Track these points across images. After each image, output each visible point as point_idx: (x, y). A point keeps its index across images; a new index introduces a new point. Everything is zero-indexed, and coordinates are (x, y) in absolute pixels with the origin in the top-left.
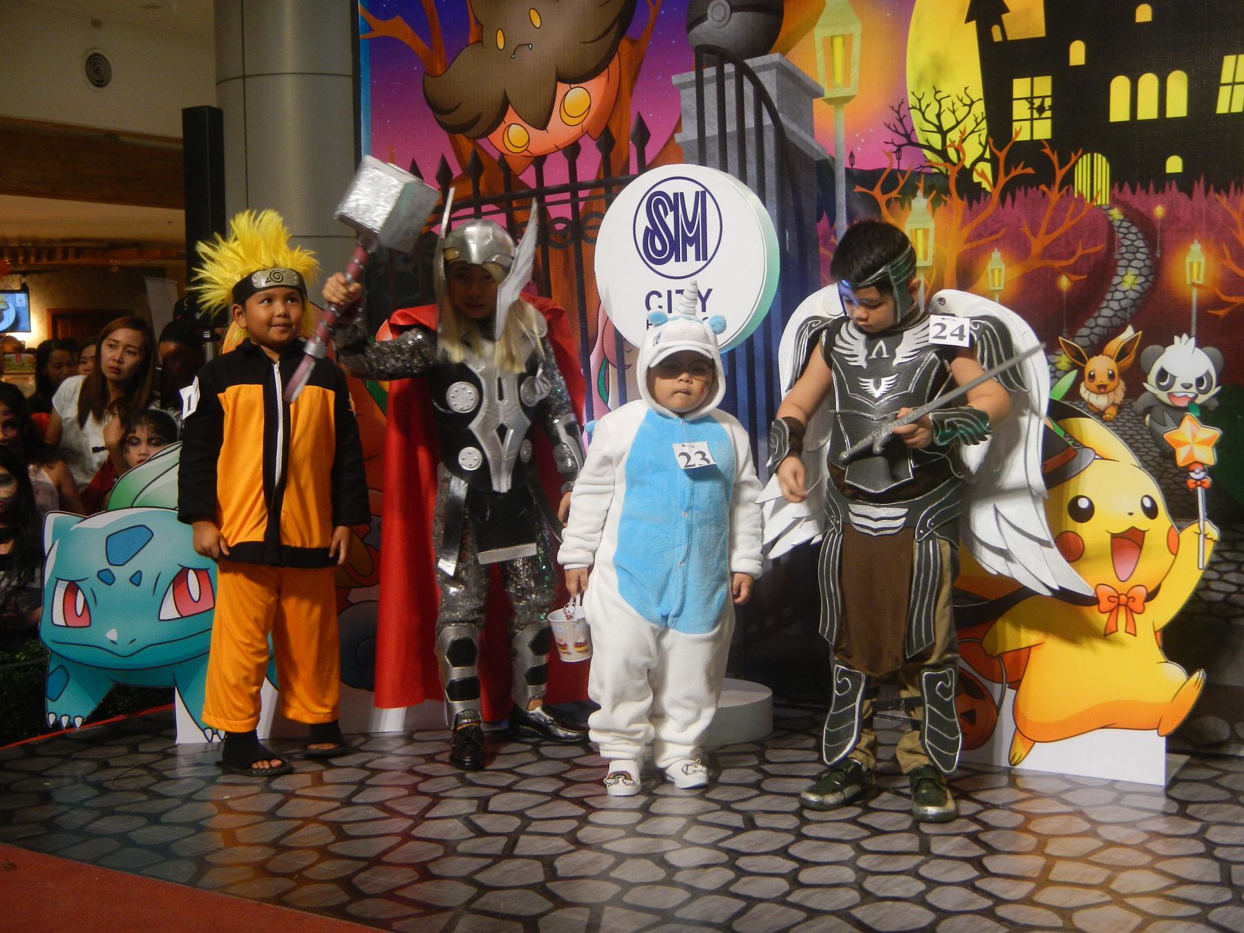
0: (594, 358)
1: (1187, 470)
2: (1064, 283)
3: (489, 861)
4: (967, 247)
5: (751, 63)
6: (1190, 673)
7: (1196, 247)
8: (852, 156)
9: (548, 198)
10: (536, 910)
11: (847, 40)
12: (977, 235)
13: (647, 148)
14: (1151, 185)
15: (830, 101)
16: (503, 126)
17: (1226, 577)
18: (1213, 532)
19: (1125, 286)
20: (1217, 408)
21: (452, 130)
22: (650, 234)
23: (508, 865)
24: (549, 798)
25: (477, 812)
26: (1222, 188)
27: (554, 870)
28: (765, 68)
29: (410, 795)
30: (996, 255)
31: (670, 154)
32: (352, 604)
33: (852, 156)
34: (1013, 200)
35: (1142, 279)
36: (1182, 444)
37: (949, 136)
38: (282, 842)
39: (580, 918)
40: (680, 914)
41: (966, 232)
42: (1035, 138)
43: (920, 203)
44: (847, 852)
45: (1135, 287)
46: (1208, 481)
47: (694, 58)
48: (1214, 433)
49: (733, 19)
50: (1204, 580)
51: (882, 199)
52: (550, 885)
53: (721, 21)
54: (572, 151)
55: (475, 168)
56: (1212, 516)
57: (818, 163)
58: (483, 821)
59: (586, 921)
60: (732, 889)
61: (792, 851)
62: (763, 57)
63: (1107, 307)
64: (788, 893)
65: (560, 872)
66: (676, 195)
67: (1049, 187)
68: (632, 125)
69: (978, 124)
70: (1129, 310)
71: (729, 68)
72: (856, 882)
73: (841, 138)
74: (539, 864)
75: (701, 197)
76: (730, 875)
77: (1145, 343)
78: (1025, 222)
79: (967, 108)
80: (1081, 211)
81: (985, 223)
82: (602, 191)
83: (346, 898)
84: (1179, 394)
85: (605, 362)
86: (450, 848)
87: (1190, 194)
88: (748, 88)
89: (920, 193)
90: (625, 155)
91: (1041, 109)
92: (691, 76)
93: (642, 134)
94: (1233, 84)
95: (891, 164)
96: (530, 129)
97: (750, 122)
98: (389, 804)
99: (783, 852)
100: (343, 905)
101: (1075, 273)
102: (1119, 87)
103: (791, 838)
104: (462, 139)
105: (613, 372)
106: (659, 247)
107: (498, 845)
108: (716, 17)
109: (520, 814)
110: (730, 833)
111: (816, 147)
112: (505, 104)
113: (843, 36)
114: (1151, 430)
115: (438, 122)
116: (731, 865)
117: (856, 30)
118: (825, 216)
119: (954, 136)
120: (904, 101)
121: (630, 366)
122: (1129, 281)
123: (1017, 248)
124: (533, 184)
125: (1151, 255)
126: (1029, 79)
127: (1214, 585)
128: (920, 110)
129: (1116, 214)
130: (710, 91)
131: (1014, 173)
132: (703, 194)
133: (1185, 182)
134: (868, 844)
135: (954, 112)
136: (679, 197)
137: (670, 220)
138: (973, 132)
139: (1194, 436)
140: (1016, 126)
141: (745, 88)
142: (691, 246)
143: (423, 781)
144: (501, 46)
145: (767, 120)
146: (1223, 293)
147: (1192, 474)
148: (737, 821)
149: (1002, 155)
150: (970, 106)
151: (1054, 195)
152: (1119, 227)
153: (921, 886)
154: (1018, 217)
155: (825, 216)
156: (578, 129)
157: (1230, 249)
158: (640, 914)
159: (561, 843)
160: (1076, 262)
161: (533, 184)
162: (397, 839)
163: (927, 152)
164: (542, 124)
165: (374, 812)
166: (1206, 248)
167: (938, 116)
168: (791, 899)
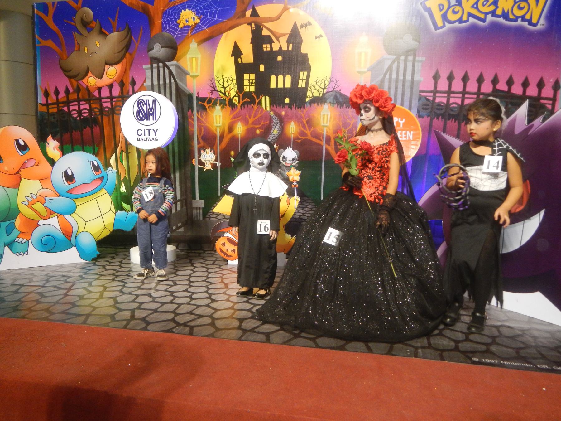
0: (118, 150)
1: (292, 183)
2: (258, 132)
3: (95, 300)
4: (232, 120)
5: (168, 63)
6: (292, 237)
7: (293, 123)
8: (198, 93)
9: (103, 101)
10: (114, 313)
11: (197, 59)
12: (234, 117)
13: (135, 87)
14: (281, 106)
15: (192, 76)
16: (87, 77)
17: (299, 211)
18: (298, 199)
19: (274, 133)
20: (298, 167)
21: (70, 77)
22: (139, 112)
23: (101, 301)
24: (111, 281)
25: (89, 286)
26: (300, 107)
27: (117, 301)
28: (172, 65)
29: (64, 283)
30: (239, 123)
31: (142, 88)
32: (40, 225)
33: (198, 93)
34: (244, 108)
35: (279, 131)
36: (291, 175)
37: (226, 89)
38: (22, 300)
39: (128, 314)
40: (159, 310)
41: (231, 116)
42: (250, 91)
43: (218, 107)
44: (205, 289)
46: (297, 185)
48: (299, 172)
49: (162, 50)
50: (295, 212)
51: (207, 106)
52: (117, 305)
54: (111, 86)
55: (78, 90)
56: (298, 195)
57: (188, 94)
58: (90, 289)
59: (130, 314)
60: (173, 302)
61: (189, 290)
63: (269, 139)
64: (190, 301)
65: (119, 302)
66: (146, 100)
67: (254, 105)
68: (130, 80)
69: (234, 86)
71: (161, 65)
72: (209, 297)
73: (195, 87)
74: (111, 299)
75: (155, 101)
76: (172, 298)
77: (279, 149)
78: (247, 114)
79: (231, 81)
80: (262, 112)
81: (236, 114)
82: (120, 99)
83: (48, 315)
84: (288, 163)
85: (122, 151)
86: (81, 297)
87: (291, 108)
88: (167, 71)
89: (218, 105)
90: (128, 89)
91: (252, 83)
92: (149, 66)
93: (134, 83)
94: (303, 79)
95: (210, 95)
96: (96, 78)
97: (167, 81)
98: (58, 286)
99: (186, 290)
100: (48, 317)
101: (261, 129)
102: (273, 78)
103: (188, 287)
104: (73, 80)
105: (124, 154)
106: (141, 116)
107: (98, 295)
109: (103, 286)
110: (170, 286)
111: (188, 90)
112: (88, 70)
113: (195, 58)
114: (281, 173)
115: (64, 74)
116: (172, 295)
117: (199, 56)
118: (190, 110)
119: (228, 89)
120: (213, 78)
121: (130, 153)
122: (275, 132)
123: (246, 122)
124: (98, 96)
125: (281, 125)
126: (248, 74)
127: (297, 214)
128: (218, 81)
129: (272, 113)
130: (155, 71)
131: (244, 100)
132: (155, 101)
133: (290, 105)
134: (210, 287)
135: (228, 82)
136: (147, 101)
137: (144, 108)
138: (233, 88)
139: (294, 173)
140: (245, 87)
141: (166, 71)
143: (68, 278)
144: (86, 52)
145: (173, 81)
146: (300, 135)
147: (293, 183)
148: (171, 283)
149: (241, 95)
150: (232, 81)
151: (255, 107)
152: (273, 117)
153: (228, 297)
154: (246, 114)
155: (190, 110)
156: (112, 80)
157: (301, 124)
158: (147, 311)
159: (118, 293)
160: (261, 126)
161: (98, 96)
162: (62, 296)
163: (220, 93)
164: (101, 77)
165: (53, 289)
166: (295, 124)
167: (223, 83)
168: (192, 302)
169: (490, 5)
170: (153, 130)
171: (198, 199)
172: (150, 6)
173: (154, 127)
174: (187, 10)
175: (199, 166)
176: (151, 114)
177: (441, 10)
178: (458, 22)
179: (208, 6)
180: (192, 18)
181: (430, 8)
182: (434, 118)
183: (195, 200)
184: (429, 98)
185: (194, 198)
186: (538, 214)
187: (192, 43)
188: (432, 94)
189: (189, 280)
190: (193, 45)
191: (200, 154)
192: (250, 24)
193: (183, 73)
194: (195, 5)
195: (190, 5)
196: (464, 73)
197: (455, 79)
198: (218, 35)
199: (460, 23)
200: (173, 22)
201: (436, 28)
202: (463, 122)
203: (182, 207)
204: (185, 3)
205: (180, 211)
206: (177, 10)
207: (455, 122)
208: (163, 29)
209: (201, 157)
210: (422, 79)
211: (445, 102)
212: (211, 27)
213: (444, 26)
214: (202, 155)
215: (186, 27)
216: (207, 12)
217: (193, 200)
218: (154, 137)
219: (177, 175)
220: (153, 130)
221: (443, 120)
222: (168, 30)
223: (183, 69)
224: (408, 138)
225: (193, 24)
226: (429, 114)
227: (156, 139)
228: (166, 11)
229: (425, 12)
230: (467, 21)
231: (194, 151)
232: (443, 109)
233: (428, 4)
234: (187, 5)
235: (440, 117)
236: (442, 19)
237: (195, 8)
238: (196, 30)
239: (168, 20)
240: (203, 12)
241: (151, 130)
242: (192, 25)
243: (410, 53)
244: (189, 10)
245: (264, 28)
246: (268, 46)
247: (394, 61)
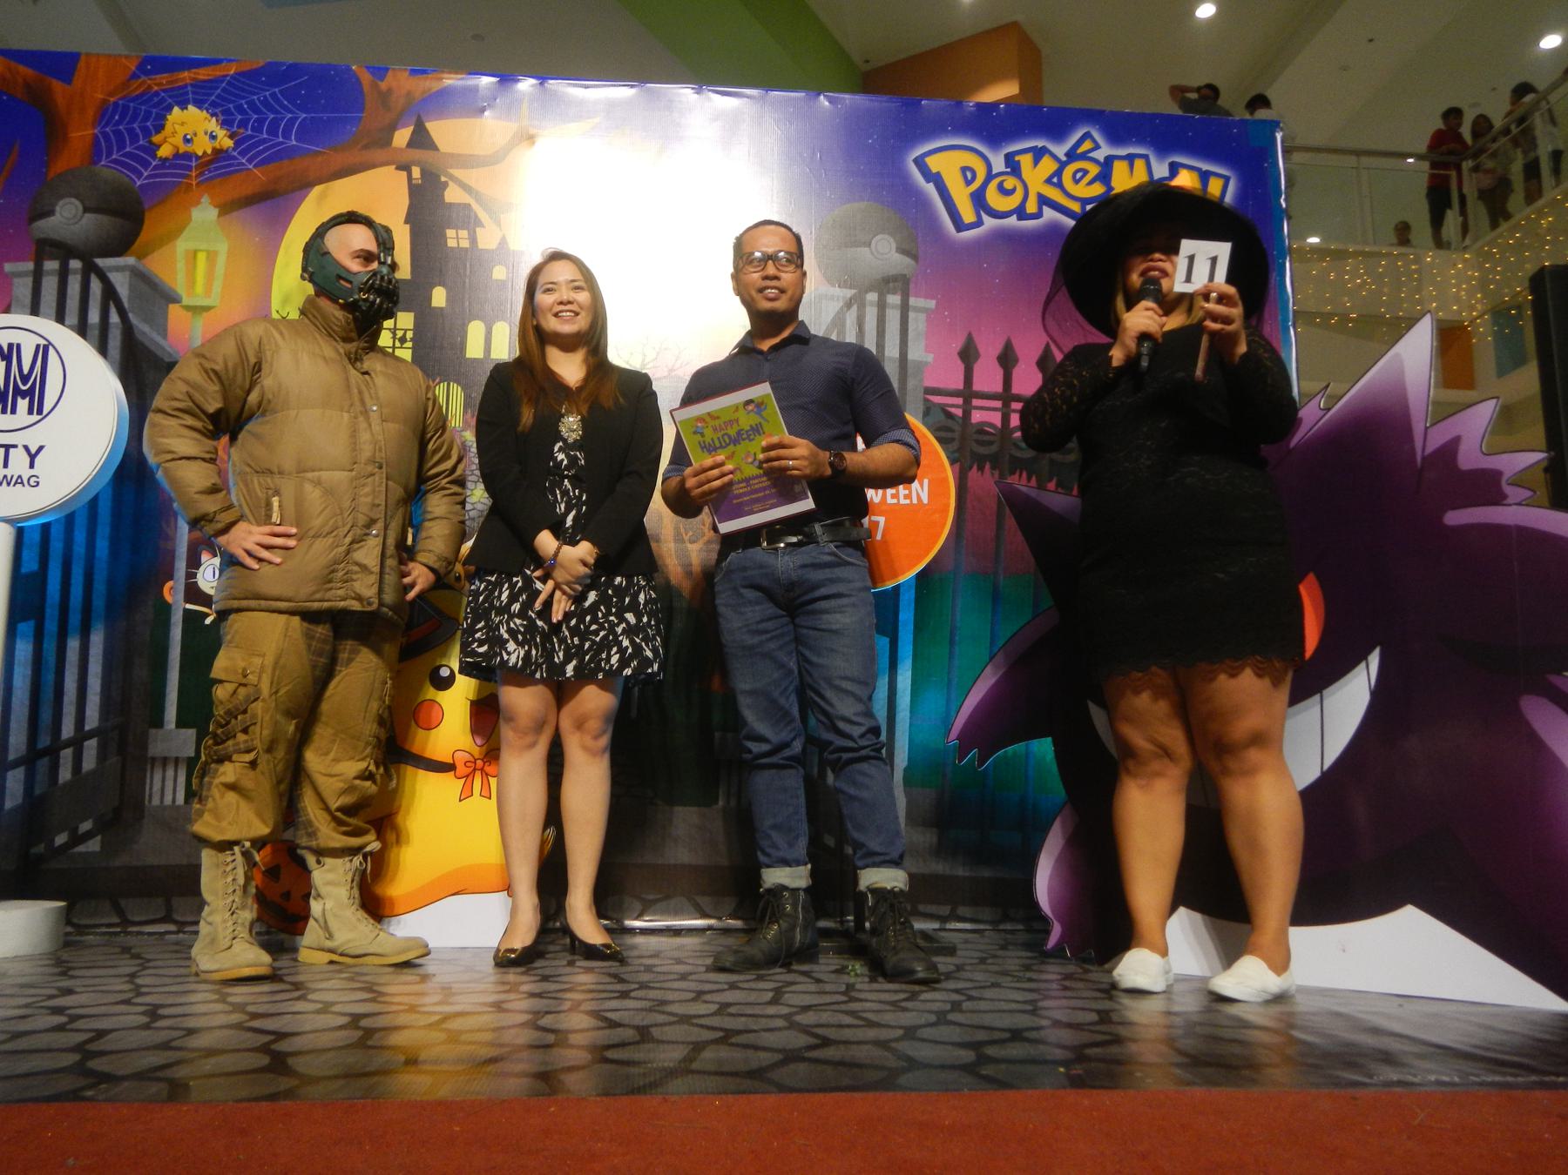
5: (100, 262)
11: (212, 257)
15: (188, 308)
28: (118, 269)
45: (482, 500)
47: (34, 248)
49: (84, 221)
53: (67, 219)
62: (117, 259)
66: (10, 346)
70: (477, 520)
75: (43, 351)
88: (96, 286)
92: (30, 266)
97: (94, 317)
99: (127, 1002)
102: (475, 331)
108: (65, 214)
111: (168, 349)
113: (208, 252)
117: (222, 248)
132: (46, 349)
141: (92, 285)
142: (23, 398)
145: (114, 318)
169: (1091, 183)
170: (26, 448)
171: (173, 726)
172: (57, 86)
173: (32, 439)
174: (191, 107)
175: (189, 606)
176: (24, 394)
177: (968, 183)
178: (1015, 216)
179: (265, 103)
180: (206, 133)
181: (938, 174)
182: (971, 468)
183: (160, 732)
184: (953, 410)
185: (158, 722)
186: (1363, 665)
187: (199, 206)
188: (960, 401)
189: (132, 982)
190: (204, 213)
191: (194, 563)
192: (405, 167)
193: (158, 295)
194: (217, 97)
195: (204, 94)
196: (1043, 346)
197: (1019, 364)
198: (293, 191)
199: (1020, 219)
200: (134, 138)
201: (959, 225)
202: (1050, 480)
203: (102, 755)
204: (185, 86)
205: (92, 773)
206: (154, 106)
207: (1029, 480)
208: (95, 153)
209: (199, 576)
210: (930, 358)
211: (999, 425)
212: (271, 167)
213: (979, 223)
214: (202, 569)
215: (182, 160)
216: (261, 122)
217: (153, 731)
218: (26, 475)
219: (97, 639)
220: (26, 448)
221: (996, 473)
222: (116, 162)
223: (157, 281)
224: (915, 501)
225: (209, 151)
226: (956, 455)
227: (33, 480)
228: (116, 104)
229: (928, 182)
230: (1038, 215)
231: (172, 555)
232: (991, 443)
233: (934, 163)
234: (193, 93)
235: (988, 466)
236: (974, 206)
237: (223, 106)
238: (216, 169)
239: (118, 133)
240: (249, 119)
241: (15, 446)
242: (205, 153)
243: (891, 285)
244: (200, 108)
245: (451, 183)
246: (464, 233)
247: (849, 305)
